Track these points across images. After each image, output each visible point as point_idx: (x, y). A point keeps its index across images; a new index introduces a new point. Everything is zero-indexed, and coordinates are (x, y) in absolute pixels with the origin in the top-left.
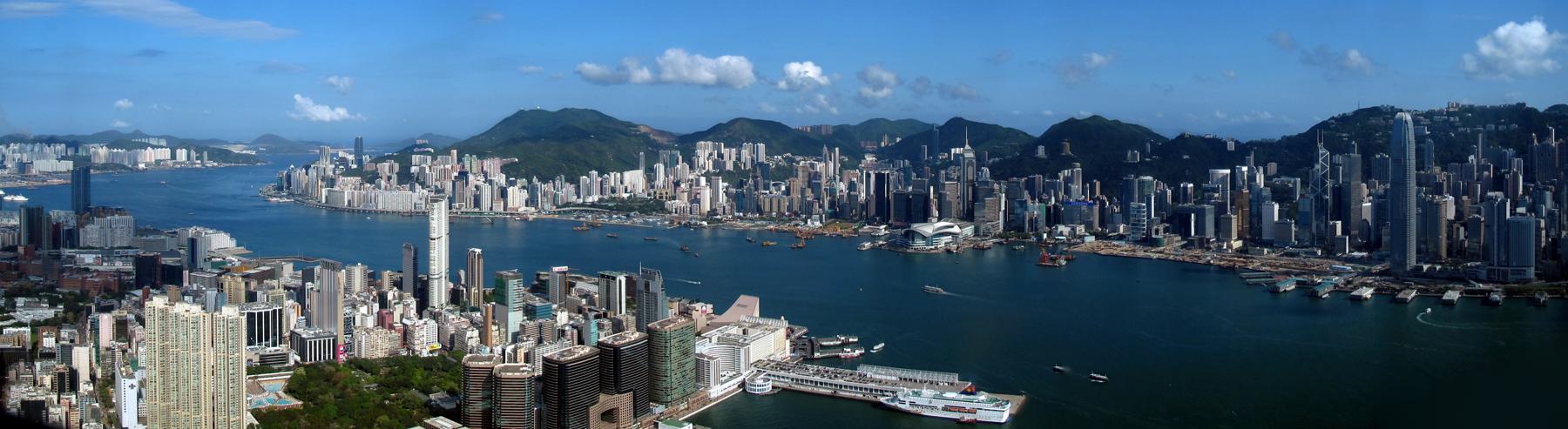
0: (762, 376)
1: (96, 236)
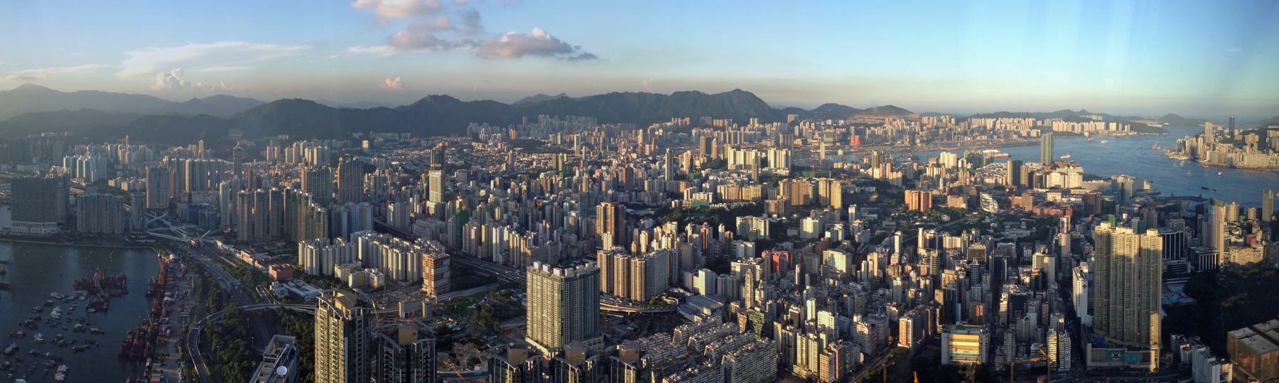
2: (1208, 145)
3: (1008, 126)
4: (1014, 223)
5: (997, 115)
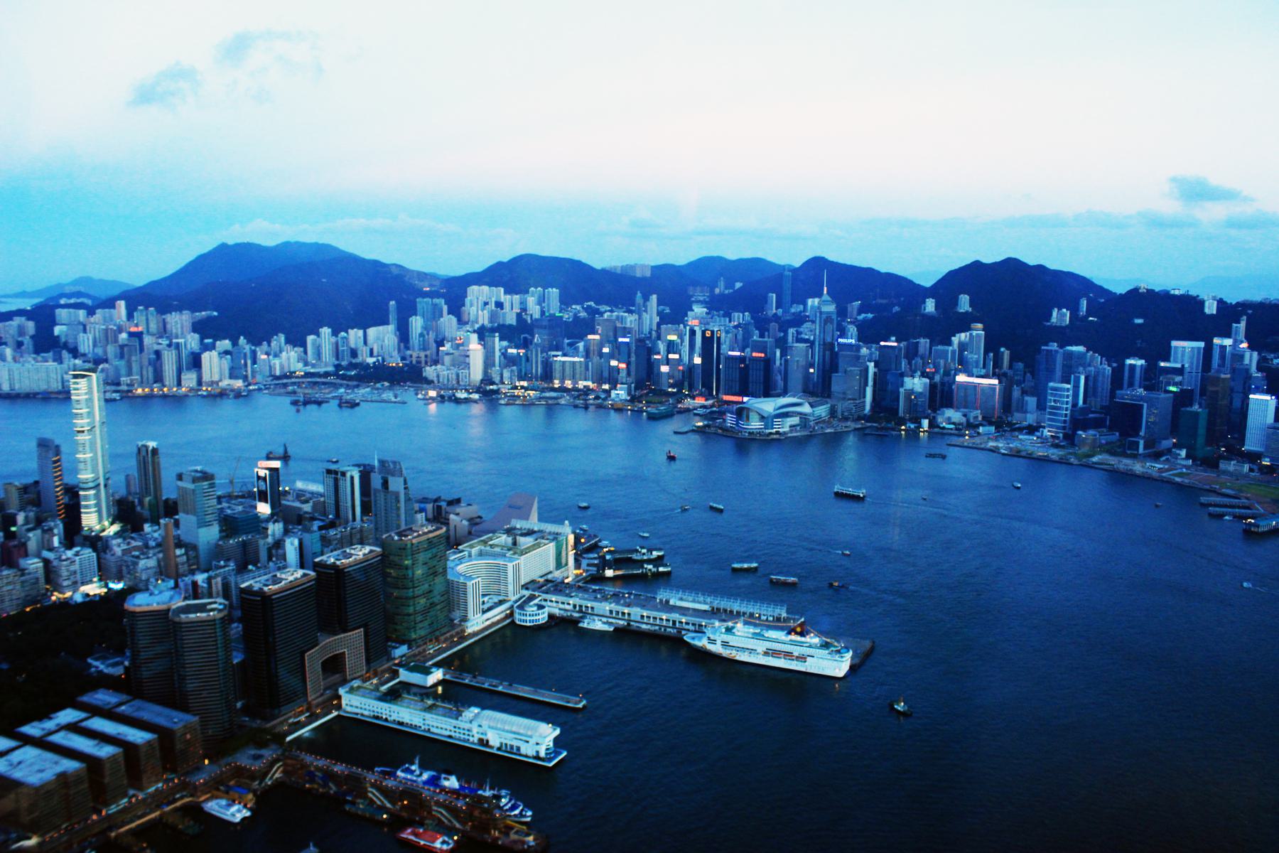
0: (536, 601)
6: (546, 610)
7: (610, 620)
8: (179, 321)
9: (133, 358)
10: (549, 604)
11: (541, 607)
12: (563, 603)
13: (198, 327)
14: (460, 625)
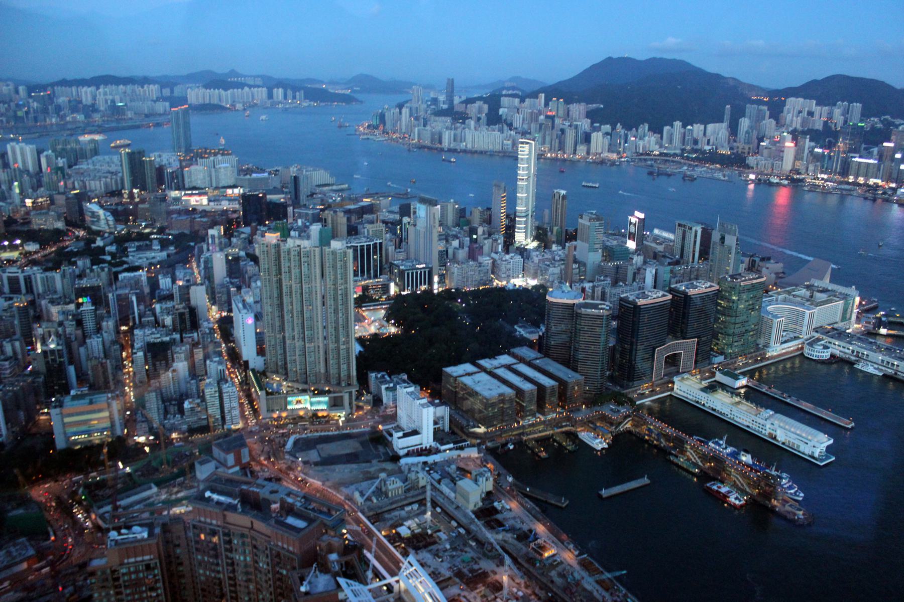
0: (822, 342)
1: (201, 176)
2: (417, 119)
3: (117, 98)
4: (141, 243)
5: (98, 82)
6: (830, 350)
7: (880, 367)
8: (579, 109)
9: (547, 133)
10: (833, 346)
11: (826, 347)
12: (844, 347)
13: (590, 115)
14: (763, 349)
